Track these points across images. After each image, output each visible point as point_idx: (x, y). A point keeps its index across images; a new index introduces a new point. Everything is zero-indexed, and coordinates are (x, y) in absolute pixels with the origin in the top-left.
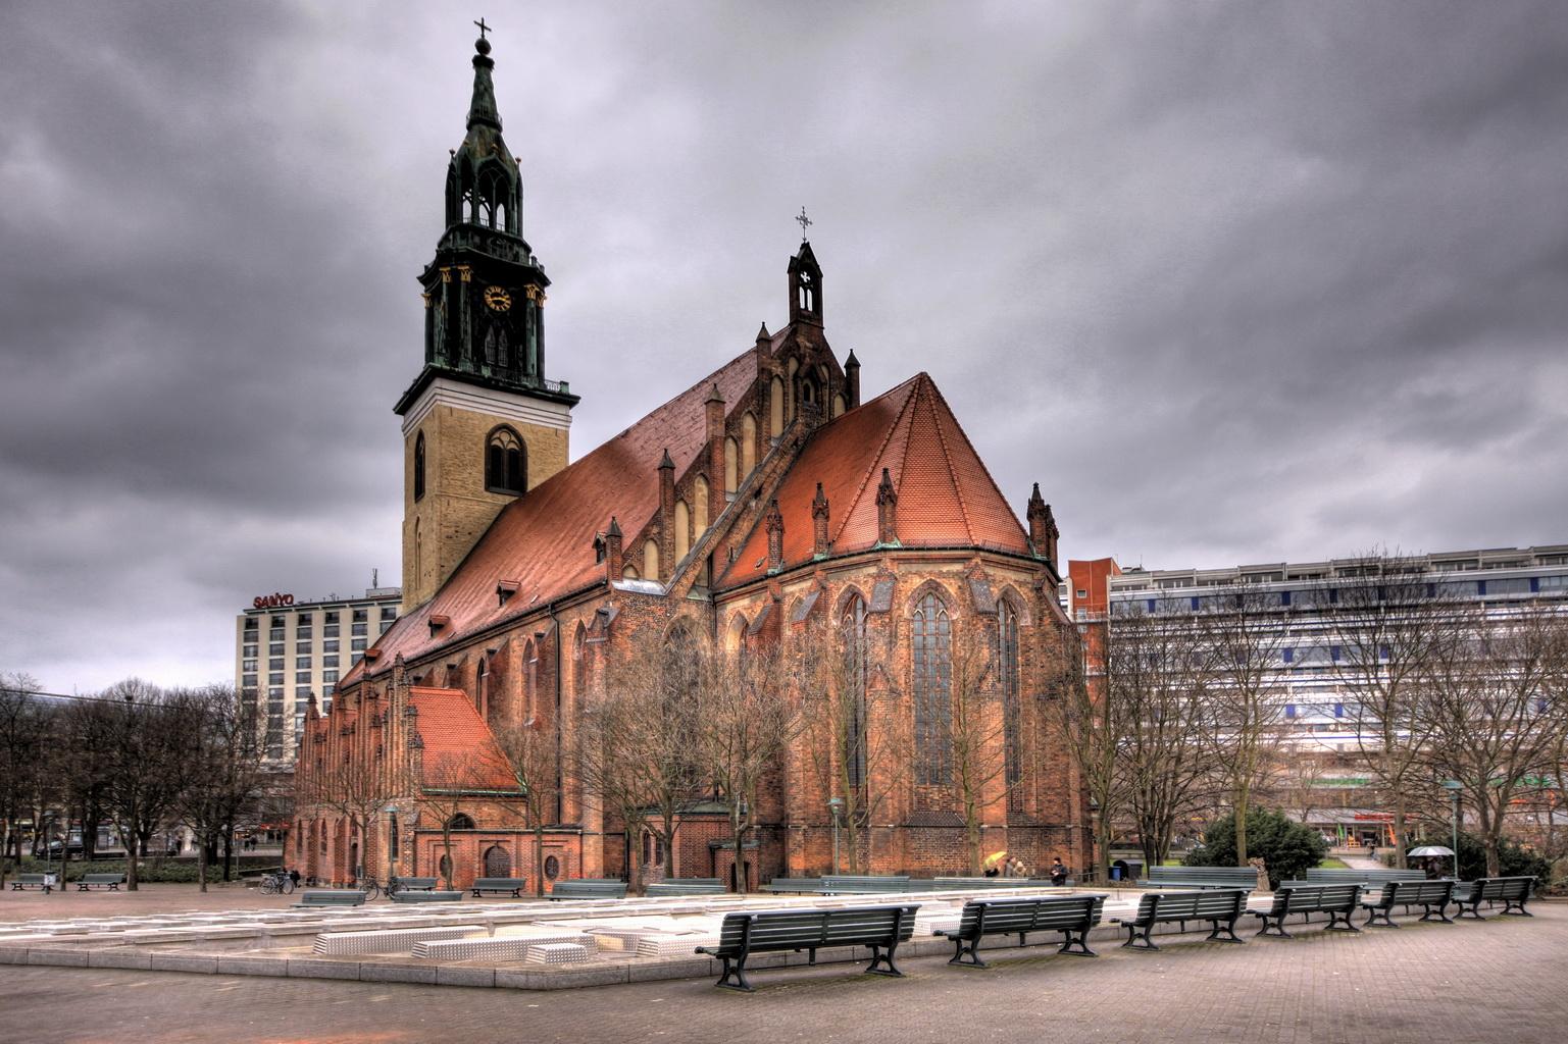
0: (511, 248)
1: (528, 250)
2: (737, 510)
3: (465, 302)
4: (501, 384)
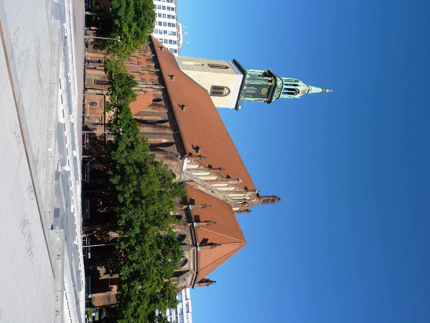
0: (278, 95)
2: (208, 187)
4: (241, 92)
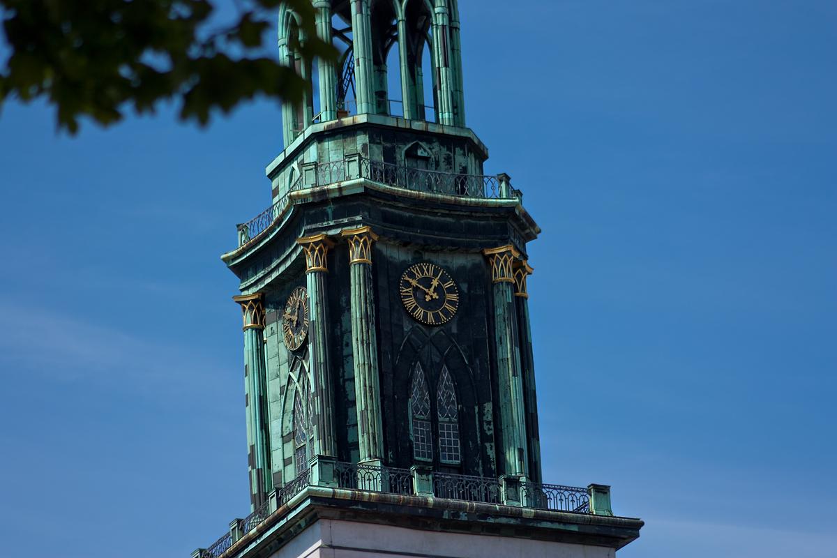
0: (449, 160)
1: (480, 154)
3: (366, 317)
4: (464, 517)
